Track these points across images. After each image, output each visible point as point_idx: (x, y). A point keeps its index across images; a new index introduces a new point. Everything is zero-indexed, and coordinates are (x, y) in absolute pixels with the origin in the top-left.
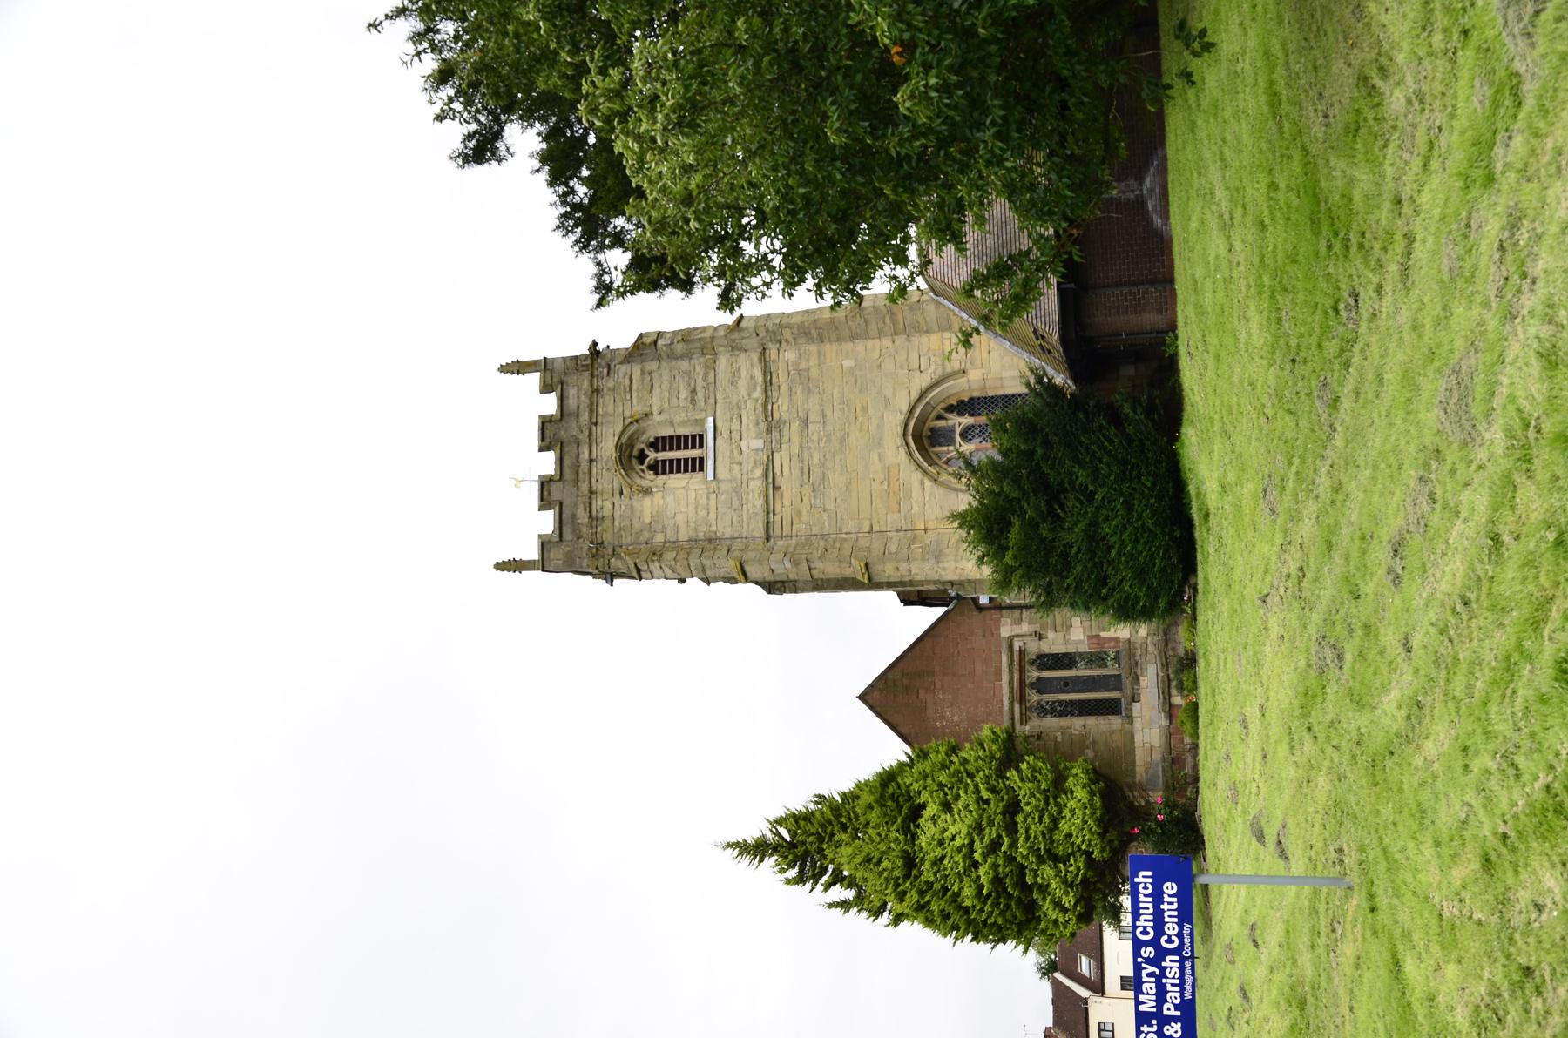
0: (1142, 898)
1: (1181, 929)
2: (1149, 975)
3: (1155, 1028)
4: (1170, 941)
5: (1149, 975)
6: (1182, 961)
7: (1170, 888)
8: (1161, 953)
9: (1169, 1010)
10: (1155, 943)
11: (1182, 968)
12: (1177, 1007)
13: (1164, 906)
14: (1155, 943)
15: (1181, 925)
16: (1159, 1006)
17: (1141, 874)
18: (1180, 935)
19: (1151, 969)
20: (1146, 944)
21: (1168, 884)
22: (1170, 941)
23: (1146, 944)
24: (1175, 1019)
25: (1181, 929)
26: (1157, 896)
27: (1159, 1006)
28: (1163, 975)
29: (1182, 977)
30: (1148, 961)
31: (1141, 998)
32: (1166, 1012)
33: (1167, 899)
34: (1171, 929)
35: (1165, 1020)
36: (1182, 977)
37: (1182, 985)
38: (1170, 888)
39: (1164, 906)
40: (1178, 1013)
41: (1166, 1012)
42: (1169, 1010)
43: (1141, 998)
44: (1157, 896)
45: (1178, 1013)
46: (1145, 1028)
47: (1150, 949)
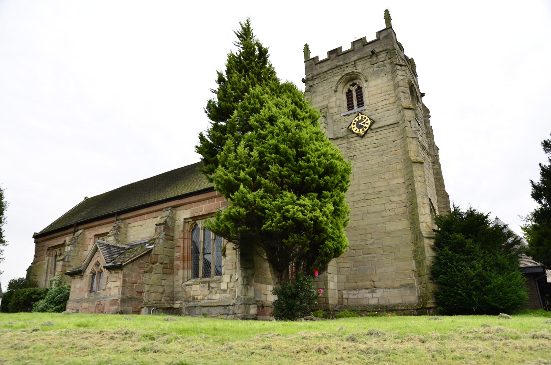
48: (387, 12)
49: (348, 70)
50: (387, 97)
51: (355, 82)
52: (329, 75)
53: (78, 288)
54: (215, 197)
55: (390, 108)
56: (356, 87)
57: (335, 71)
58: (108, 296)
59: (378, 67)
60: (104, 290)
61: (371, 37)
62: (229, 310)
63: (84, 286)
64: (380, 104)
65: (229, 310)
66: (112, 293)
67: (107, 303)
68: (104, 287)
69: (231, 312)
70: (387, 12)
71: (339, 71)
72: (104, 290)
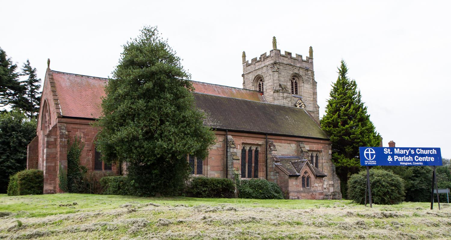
0: (428, 151)
1: (421, 162)
2: (406, 152)
3: (389, 153)
4: (417, 158)
5: (406, 152)
6: (412, 162)
7: (432, 159)
8: (413, 156)
9: (396, 158)
10: (415, 154)
11: (409, 162)
12: (397, 160)
13: (427, 157)
14: (415, 154)
15: (422, 162)
16: (396, 155)
17: (435, 151)
18: (419, 162)
19: (408, 153)
20: (415, 151)
21: (433, 159)
22: (417, 158)
23: (415, 151)
24: (393, 159)
25: (421, 162)
26: (429, 155)
27: (396, 155)
28: (408, 156)
29: (406, 162)
30: (410, 152)
31: (398, 149)
32: (395, 157)
33: (429, 158)
34: (420, 159)
35: (392, 156)
36: (406, 162)
37: (404, 161)
38: (432, 159)
39: (427, 157)
40: (395, 160)
41: (395, 157)
42: (396, 158)
43: (398, 149)
44: (429, 155)
45: (395, 160)
46: (389, 150)
47: (414, 153)
48: (311, 48)
49: (296, 71)
50: (310, 96)
51: (295, 78)
52: (288, 67)
53: (294, 185)
54: (320, 143)
55: (311, 103)
56: (295, 81)
57: (291, 67)
58: (316, 190)
59: (308, 78)
60: (313, 187)
61: (304, 58)
62: (329, 197)
63: (299, 184)
64: (308, 99)
65: (329, 197)
66: (318, 189)
67: (317, 194)
68: (313, 186)
69: (329, 198)
70: (311, 48)
71: (292, 68)
72: (313, 187)
